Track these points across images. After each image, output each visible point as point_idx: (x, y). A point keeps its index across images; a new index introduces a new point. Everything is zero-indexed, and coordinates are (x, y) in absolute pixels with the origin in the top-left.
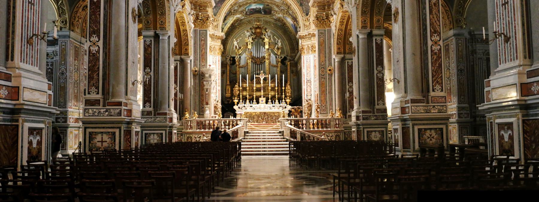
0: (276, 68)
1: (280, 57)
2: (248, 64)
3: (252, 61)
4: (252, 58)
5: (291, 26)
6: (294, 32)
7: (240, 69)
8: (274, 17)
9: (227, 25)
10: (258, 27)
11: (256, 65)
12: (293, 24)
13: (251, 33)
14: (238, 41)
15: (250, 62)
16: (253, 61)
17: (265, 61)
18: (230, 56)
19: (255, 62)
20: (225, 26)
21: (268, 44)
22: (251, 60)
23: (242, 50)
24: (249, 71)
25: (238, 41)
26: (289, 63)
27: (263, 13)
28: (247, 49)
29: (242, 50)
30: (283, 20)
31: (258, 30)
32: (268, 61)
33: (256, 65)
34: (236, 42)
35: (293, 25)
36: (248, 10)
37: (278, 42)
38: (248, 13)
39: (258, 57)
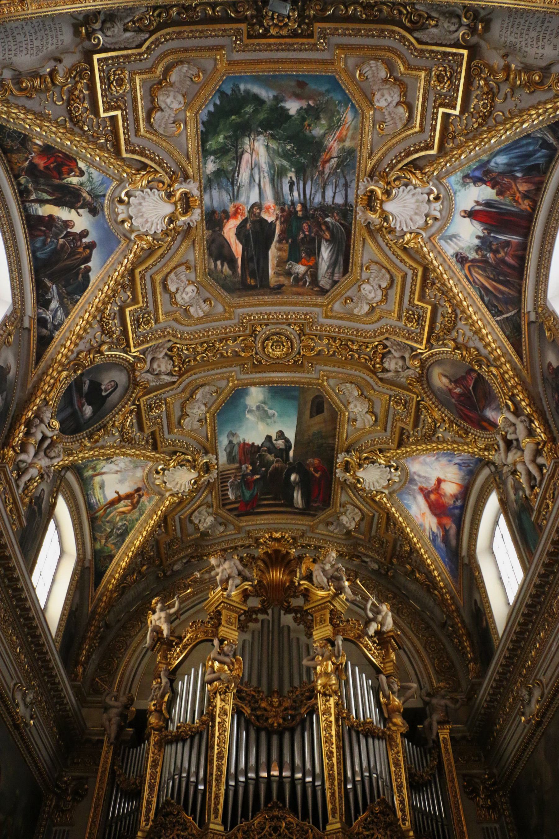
0: (383, 744)
1: (396, 687)
2: (213, 718)
3: (237, 711)
4: (239, 696)
5: (430, 545)
6: (447, 575)
7: (168, 749)
8: (344, 519)
9: (127, 540)
10: (277, 552)
11: (263, 735)
12: (440, 533)
13: (240, 567)
14: (172, 611)
15: (229, 708)
16: (247, 710)
17: (313, 710)
18: (123, 699)
19: (258, 718)
20: (118, 546)
21: (328, 616)
22: (230, 697)
23: (184, 648)
24: (220, 757)
25: (172, 611)
26: (444, 734)
27: (298, 496)
28: (216, 642)
29: (184, 648)
30: (389, 517)
31: (277, 575)
32: (332, 701)
33: (263, 735)
34: (163, 614)
35: (439, 540)
36: (231, 459)
37: (377, 612)
38: (231, 496)
39: (275, 687)
